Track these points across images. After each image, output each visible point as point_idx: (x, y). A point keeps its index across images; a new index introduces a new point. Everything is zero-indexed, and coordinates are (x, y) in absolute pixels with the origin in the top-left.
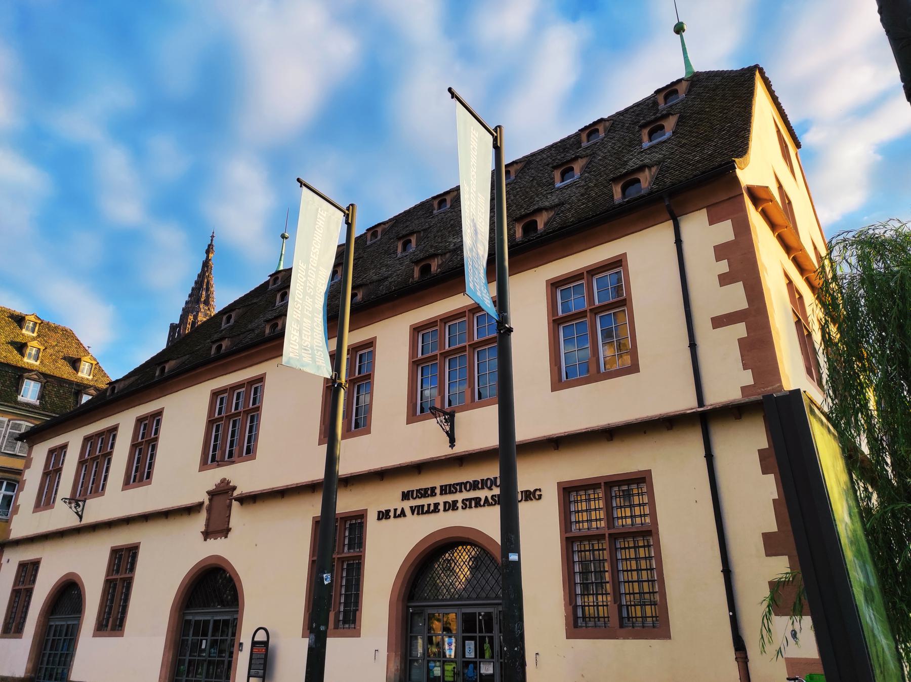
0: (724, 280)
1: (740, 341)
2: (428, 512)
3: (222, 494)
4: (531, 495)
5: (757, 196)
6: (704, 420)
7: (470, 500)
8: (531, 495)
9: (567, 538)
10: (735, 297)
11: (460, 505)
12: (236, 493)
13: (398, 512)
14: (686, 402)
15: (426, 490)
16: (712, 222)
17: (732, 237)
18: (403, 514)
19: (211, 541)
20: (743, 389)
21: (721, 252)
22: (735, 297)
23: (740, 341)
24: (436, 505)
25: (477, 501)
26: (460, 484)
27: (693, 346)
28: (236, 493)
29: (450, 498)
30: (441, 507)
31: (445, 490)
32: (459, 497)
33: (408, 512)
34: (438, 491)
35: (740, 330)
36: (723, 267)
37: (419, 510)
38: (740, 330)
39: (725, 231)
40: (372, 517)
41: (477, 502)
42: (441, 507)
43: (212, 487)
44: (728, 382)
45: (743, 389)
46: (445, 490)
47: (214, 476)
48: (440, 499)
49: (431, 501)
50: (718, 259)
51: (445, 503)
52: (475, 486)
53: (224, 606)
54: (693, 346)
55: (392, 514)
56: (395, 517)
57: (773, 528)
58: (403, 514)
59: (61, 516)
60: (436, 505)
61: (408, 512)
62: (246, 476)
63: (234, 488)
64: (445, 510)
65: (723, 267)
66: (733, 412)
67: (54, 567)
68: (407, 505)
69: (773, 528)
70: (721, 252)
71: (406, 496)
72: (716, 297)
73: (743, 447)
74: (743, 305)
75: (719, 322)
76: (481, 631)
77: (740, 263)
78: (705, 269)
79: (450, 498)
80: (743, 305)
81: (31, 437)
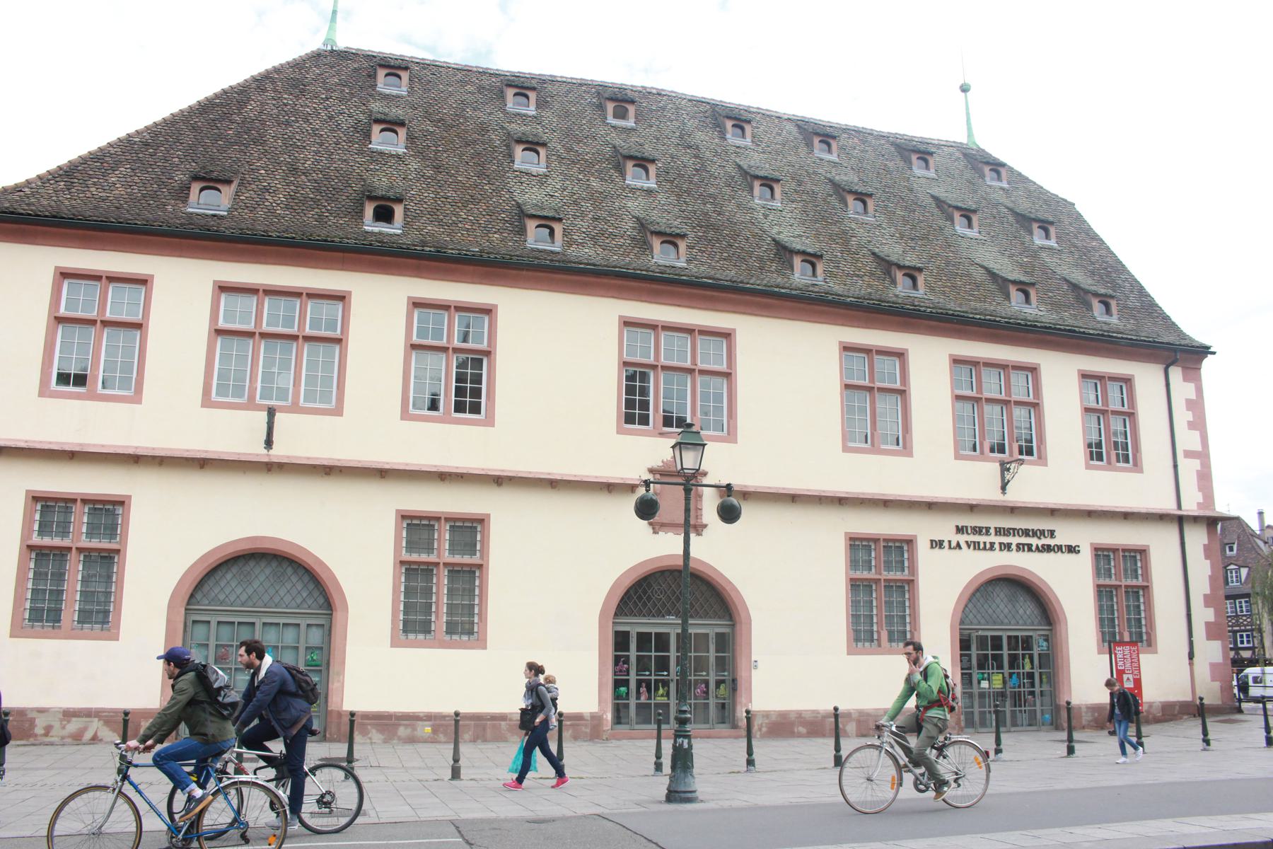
2: (985, 548)
9: (1099, 586)
11: (1014, 547)
13: (953, 544)
14: (1169, 506)
15: (981, 529)
18: (958, 546)
24: (992, 544)
25: (1030, 547)
26: (1014, 529)
27: (1175, 466)
29: (1005, 540)
30: (997, 546)
31: (999, 531)
32: (1014, 540)
33: (963, 545)
34: (992, 531)
36: (1189, 416)
37: (976, 546)
40: (922, 547)
42: (997, 546)
46: (999, 531)
48: (992, 538)
49: (988, 539)
52: (1026, 533)
54: (1175, 466)
55: (946, 544)
57: (1208, 592)
60: (992, 544)
61: (963, 545)
63: (705, 474)
65: (1189, 416)
66: (1196, 519)
68: (963, 538)
69: (1208, 592)
71: (960, 530)
73: (1197, 539)
75: (1189, 454)
79: (1005, 540)
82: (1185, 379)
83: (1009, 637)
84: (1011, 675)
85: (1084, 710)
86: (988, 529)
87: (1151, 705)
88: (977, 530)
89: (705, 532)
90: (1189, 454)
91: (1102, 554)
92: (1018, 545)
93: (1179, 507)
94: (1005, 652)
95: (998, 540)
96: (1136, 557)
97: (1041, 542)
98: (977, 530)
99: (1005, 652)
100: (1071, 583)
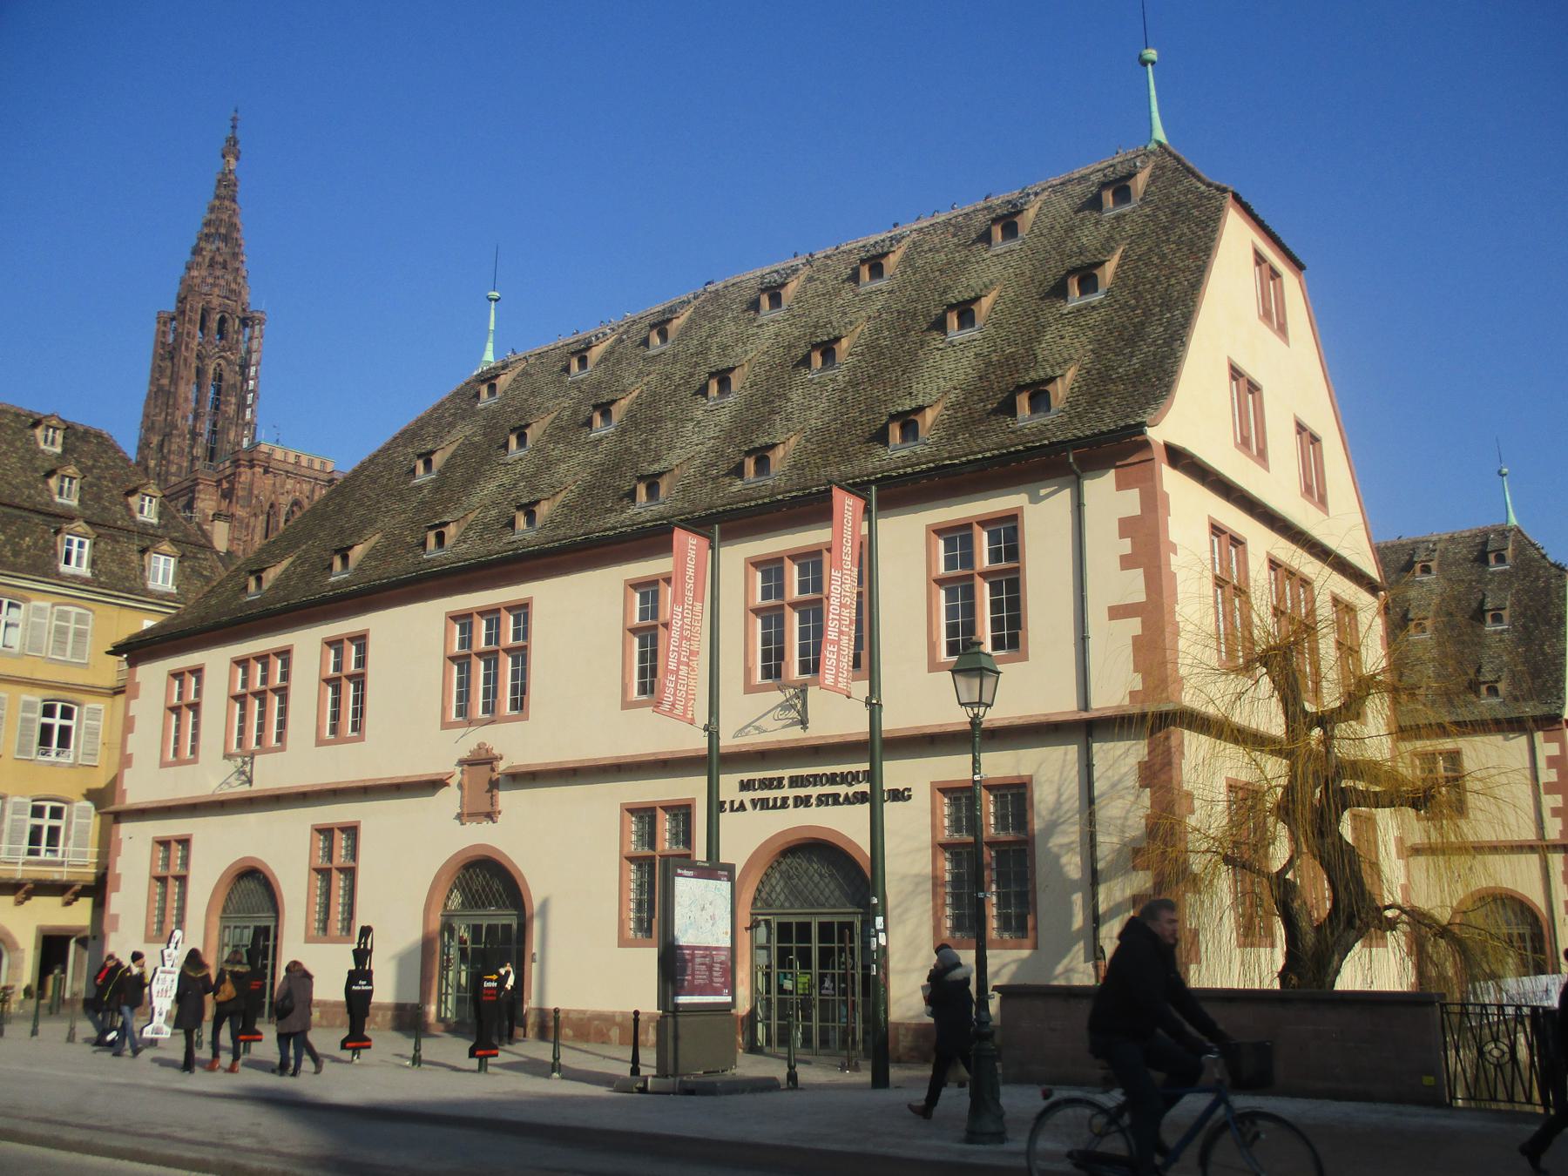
0: (1127, 562)
1: (1135, 638)
2: (775, 807)
3: (481, 761)
4: (898, 795)
5: (1178, 457)
6: (1087, 730)
7: (827, 796)
8: (898, 795)
10: (1133, 587)
12: (502, 766)
16: (1121, 485)
17: (1138, 512)
19: (472, 827)
20: (1133, 694)
21: (1127, 527)
22: (1133, 587)
23: (1135, 638)
24: (785, 800)
25: (836, 797)
28: (502, 766)
29: (802, 792)
30: (791, 802)
31: (795, 782)
32: (814, 791)
33: (748, 805)
35: (1134, 626)
36: (1126, 546)
37: (763, 804)
38: (1134, 626)
39: (1130, 502)
41: (835, 800)
42: (791, 802)
43: (465, 754)
44: (1114, 689)
45: (1133, 694)
46: (795, 782)
47: (468, 741)
50: (1122, 536)
51: (796, 798)
52: (832, 779)
53: (499, 908)
56: (732, 810)
58: (742, 807)
59: (210, 776)
60: (785, 800)
61: (748, 805)
62: (517, 744)
64: (796, 806)
65: (1126, 546)
67: (218, 847)
68: (747, 796)
70: (1127, 527)
71: (745, 786)
72: (1114, 583)
74: (1142, 598)
75: (1117, 612)
76: (841, 940)
77: (1146, 542)
78: (1106, 546)
79: (802, 792)
80: (1142, 598)
81: (137, 650)
82: (1121, 485)
83: (821, 924)
84: (822, 977)
85: (902, 1031)
86: (780, 780)
87: (897, 1025)
88: (767, 784)
89: (500, 818)
90: (1117, 612)
91: (961, 796)
92: (819, 797)
93: (1085, 705)
94: (815, 945)
95: (791, 793)
96: (1016, 795)
97: (851, 791)
98: (767, 784)
99: (815, 945)
100: (911, 847)
